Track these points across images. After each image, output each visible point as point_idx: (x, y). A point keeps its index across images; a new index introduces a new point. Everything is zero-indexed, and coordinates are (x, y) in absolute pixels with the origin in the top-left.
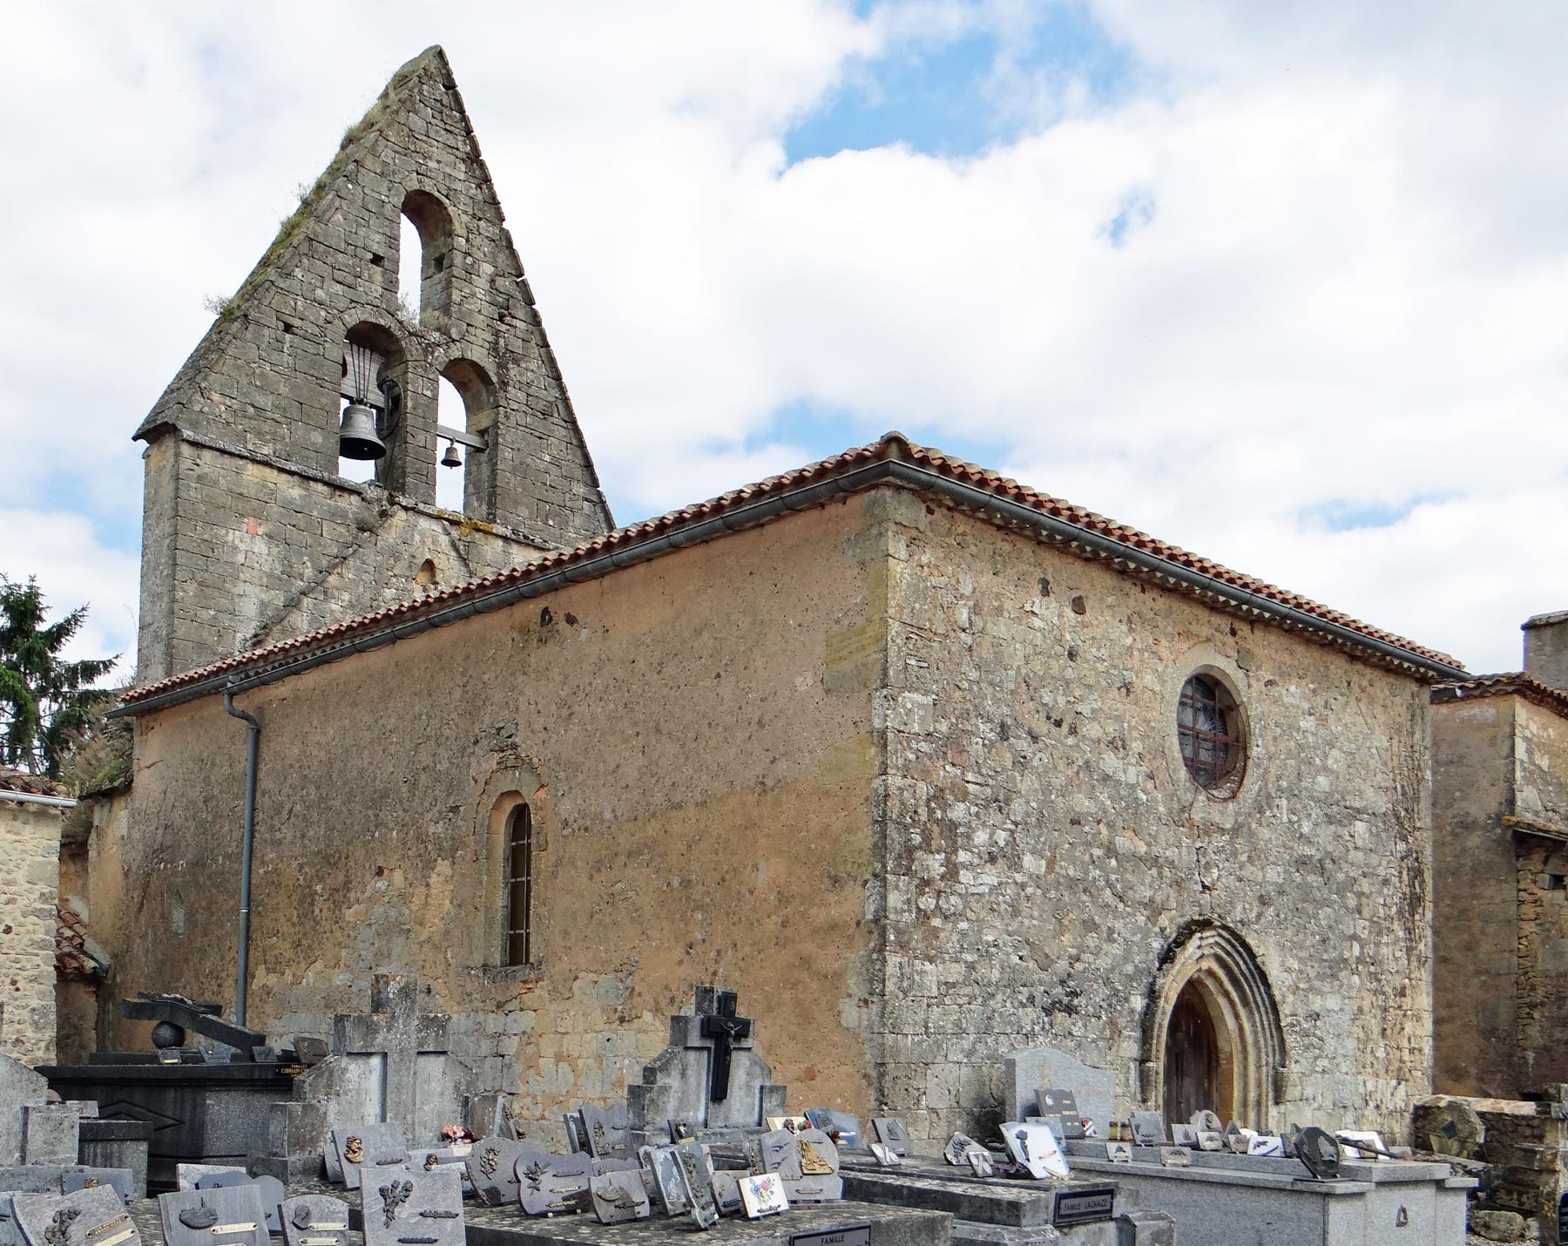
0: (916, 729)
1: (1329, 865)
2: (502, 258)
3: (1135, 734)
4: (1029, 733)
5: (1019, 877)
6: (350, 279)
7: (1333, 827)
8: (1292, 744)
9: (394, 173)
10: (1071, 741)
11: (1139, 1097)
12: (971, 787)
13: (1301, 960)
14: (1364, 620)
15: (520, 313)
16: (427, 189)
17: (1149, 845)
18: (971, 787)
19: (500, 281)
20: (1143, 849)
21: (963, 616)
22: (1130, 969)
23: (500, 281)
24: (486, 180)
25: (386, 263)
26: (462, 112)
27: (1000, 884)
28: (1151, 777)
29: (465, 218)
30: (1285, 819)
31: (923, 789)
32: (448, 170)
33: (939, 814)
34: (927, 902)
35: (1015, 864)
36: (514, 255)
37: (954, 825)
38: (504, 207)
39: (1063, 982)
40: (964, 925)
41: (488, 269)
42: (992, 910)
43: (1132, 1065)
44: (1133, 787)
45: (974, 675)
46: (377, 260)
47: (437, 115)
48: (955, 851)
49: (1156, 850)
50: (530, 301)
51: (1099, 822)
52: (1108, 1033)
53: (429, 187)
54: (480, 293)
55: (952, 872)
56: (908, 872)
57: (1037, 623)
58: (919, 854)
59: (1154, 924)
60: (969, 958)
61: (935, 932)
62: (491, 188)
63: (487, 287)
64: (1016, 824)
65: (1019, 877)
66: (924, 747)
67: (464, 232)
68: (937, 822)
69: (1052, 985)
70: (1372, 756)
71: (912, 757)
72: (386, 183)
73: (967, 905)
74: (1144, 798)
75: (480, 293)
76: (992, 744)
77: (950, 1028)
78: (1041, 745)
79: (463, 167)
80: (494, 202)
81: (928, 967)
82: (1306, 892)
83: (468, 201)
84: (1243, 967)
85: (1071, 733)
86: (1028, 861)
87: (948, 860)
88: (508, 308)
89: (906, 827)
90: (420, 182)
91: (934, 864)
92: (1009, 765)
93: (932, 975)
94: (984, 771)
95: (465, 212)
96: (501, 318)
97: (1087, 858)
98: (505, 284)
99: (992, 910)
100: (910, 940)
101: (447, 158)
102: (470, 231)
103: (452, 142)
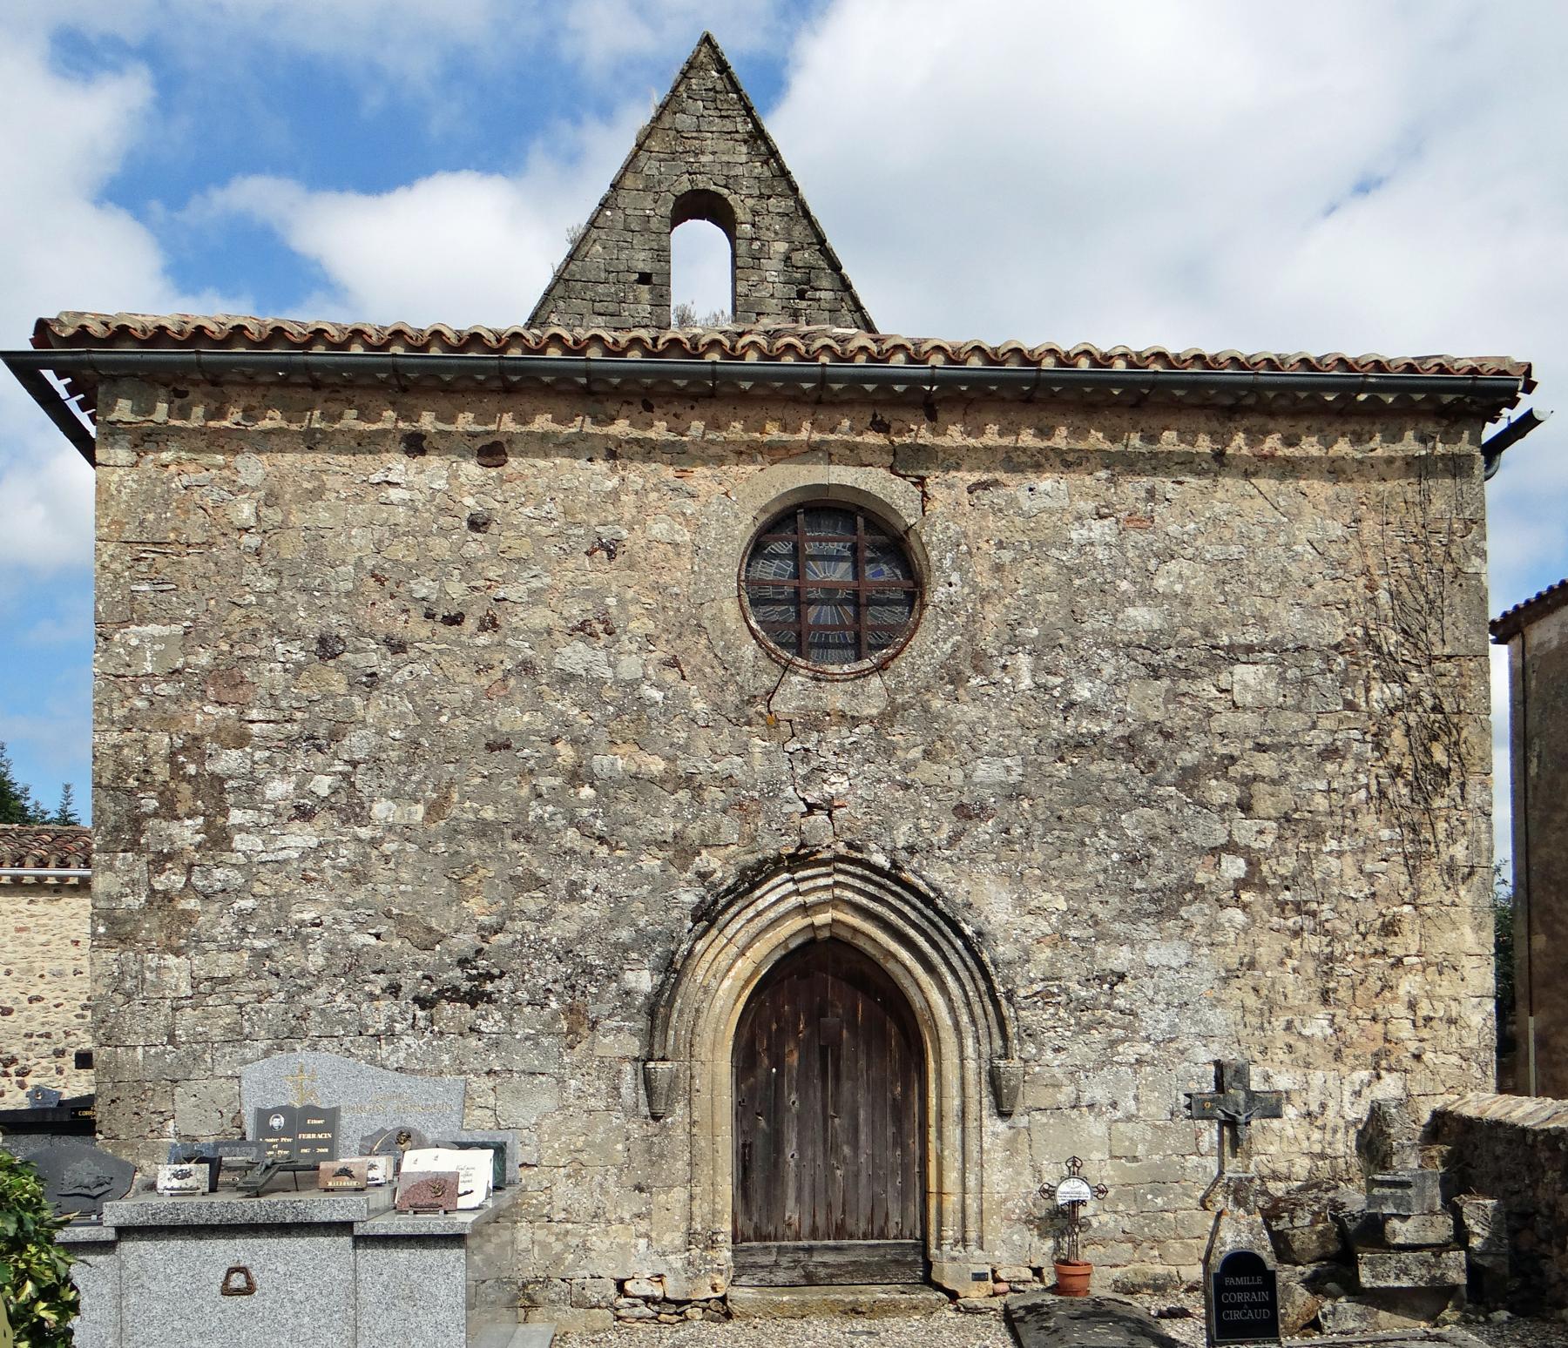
0: (149, 668)
1: (1152, 742)
2: (799, 231)
3: (634, 609)
4: (388, 641)
5: (364, 833)
6: (612, 308)
7: (1165, 683)
8: (1049, 569)
9: (660, 182)
10: (484, 639)
11: (645, 1110)
12: (255, 728)
13: (1070, 895)
14: (1246, 348)
15: (825, 283)
16: (701, 186)
17: (670, 759)
18: (255, 729)
19: (797, 257)
20: (657, 766)
21: (245, 511)
22: (625, 934)
23: (797, 257)
24: (773, 153)
25: (654, 279)
26: (738, 90)
27: (320, 845)
28: (674, 663)
29: (750, 202)
30: (1026, 682)
31: (161, 742)
32: (725, 158)
33: (192, 769)
34: (173, 879)
35: (355, 812)
36: (812, 223)
37: (218, 780)
38: (797, 177)
39: (463, 963)
40: (249, 903)
41: (781, 247)
42: (308, 880)
43: (628, 1068)
44: (634, 684)
45: (269, 583)
46: (645, 278)
47: (709, 104)
48: (225, 813)
49: (684, 765)
50: (836, 267)
51: (553, 742)
52: (564, 1025)
53: (702, 183)
54: (772, 276)
55: (218, 839)
56: (134, 846)
57: (394, 494)
58: (152, 823)
59: (684, 868)
60: (259, 944)
61: (188, 917)
62: (778, 159)
63: (781, 266)
64: (354, 764)
65: (364, 833)
66: (165, 689)
67: (749, 217)
68: (189, 779)
69: (443, 967)
70: (1296, 557)
71: (141, 704)
72: (652, 196)
73: (252, 877)
74: (658, 695)
75: (772, 276)
76: (300, 667)
77: (216, 1034)
78: (413, 653)
79: (744, 149)
80: (784, 174)
81: (171, 960)
82: (1083, 791)
83: (752, 181)
84: (913, 915)
85: (483, 628)
86: (382, 809)
87: (208, 827)
88: (808, 282)
89: (130, 792)
90: (691, 181)
91: (187, 833)
92: (342, 688)
93: (177, 972)
94: (284, 704)
95: (750, 196)
96: (801, 295)
97: (525, 791)
98: (805, 257)
99: (308, 880)
100: (138, 929)
101: (723, 145)
102: (755, 213)
103: (729, 126)
